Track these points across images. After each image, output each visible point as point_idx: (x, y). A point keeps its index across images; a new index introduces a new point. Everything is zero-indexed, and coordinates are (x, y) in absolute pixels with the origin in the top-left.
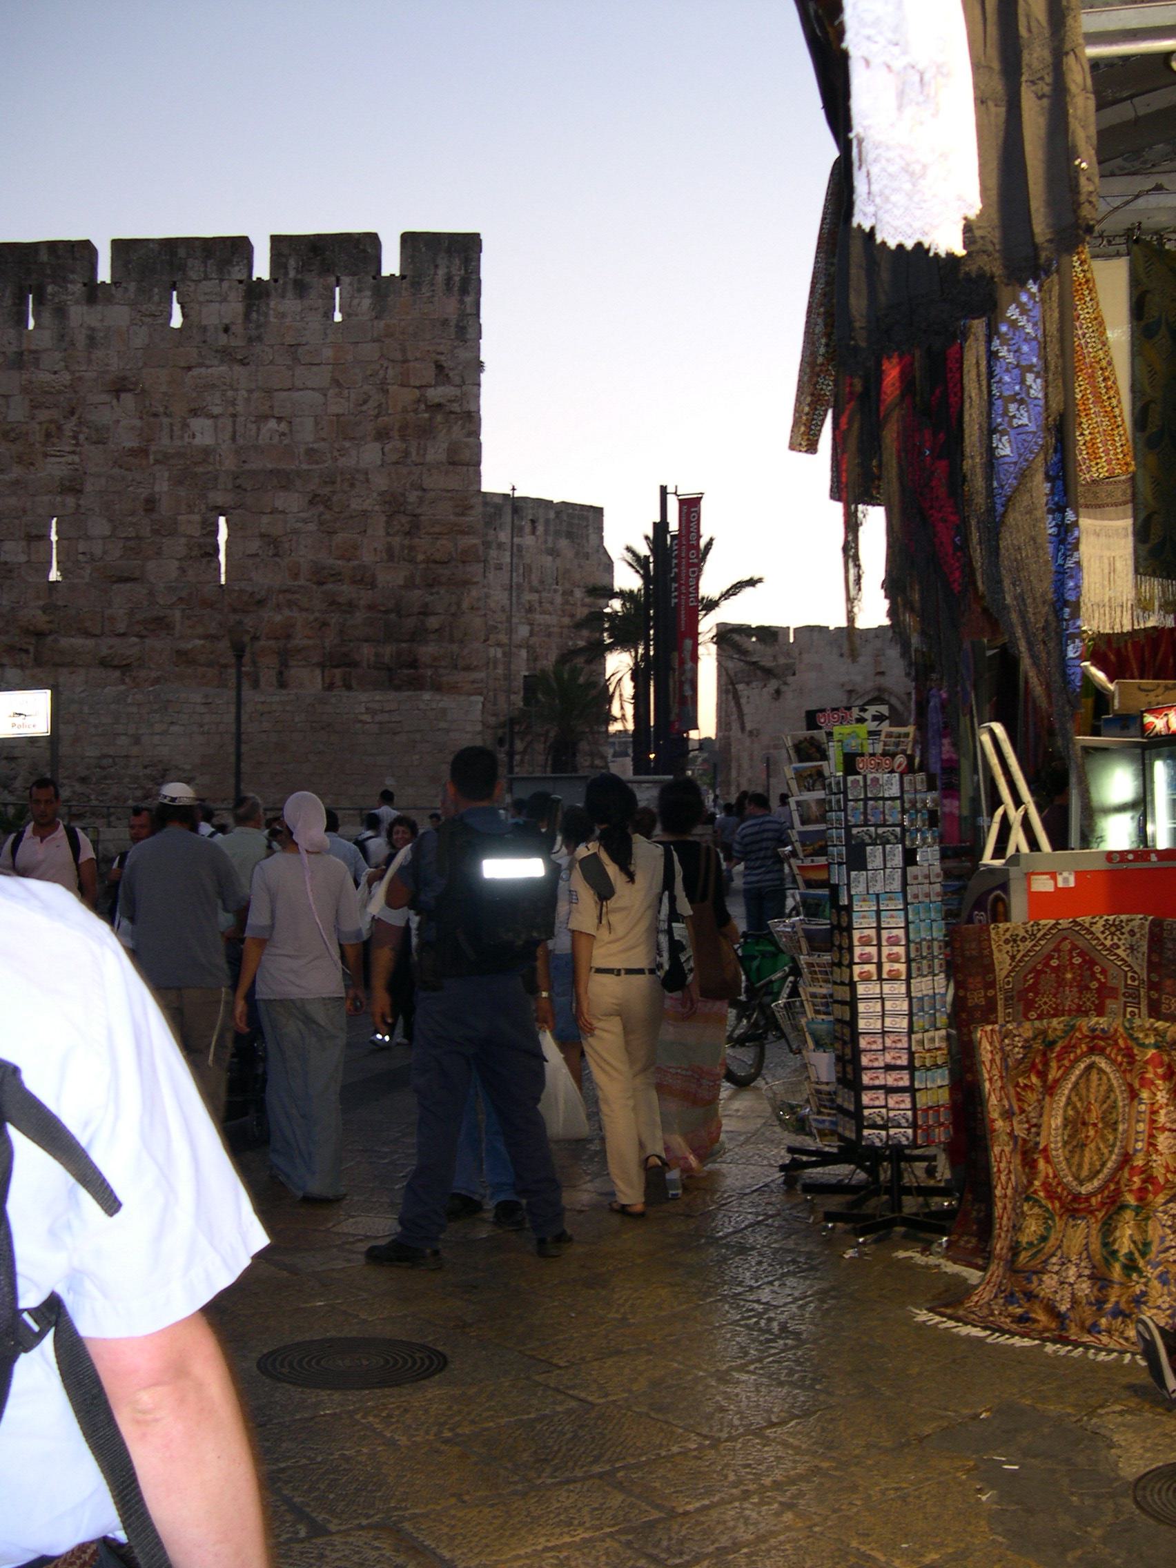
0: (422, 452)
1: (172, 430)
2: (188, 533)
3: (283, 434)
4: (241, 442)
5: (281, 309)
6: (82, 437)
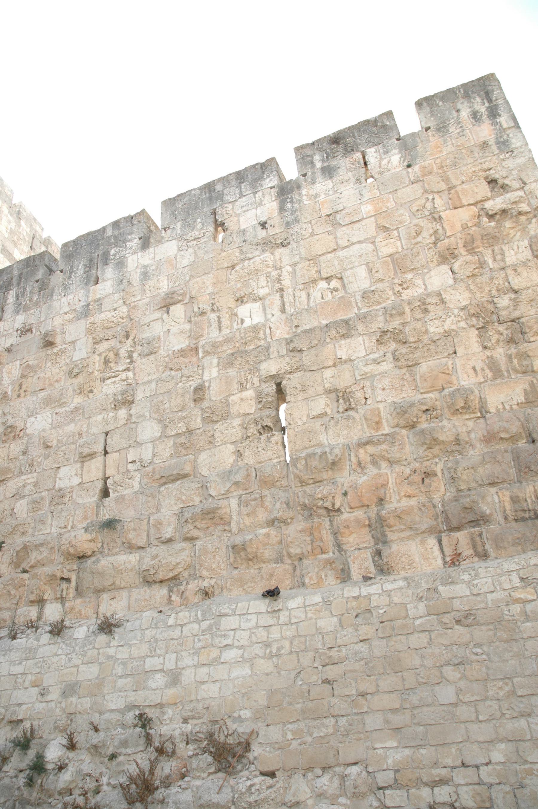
0: (499, 257)
1: (220, 322)
2: (241, 412)
3: (336, 290)
4: (290, 310)
5: (312, 192)
6: (135, 355)
